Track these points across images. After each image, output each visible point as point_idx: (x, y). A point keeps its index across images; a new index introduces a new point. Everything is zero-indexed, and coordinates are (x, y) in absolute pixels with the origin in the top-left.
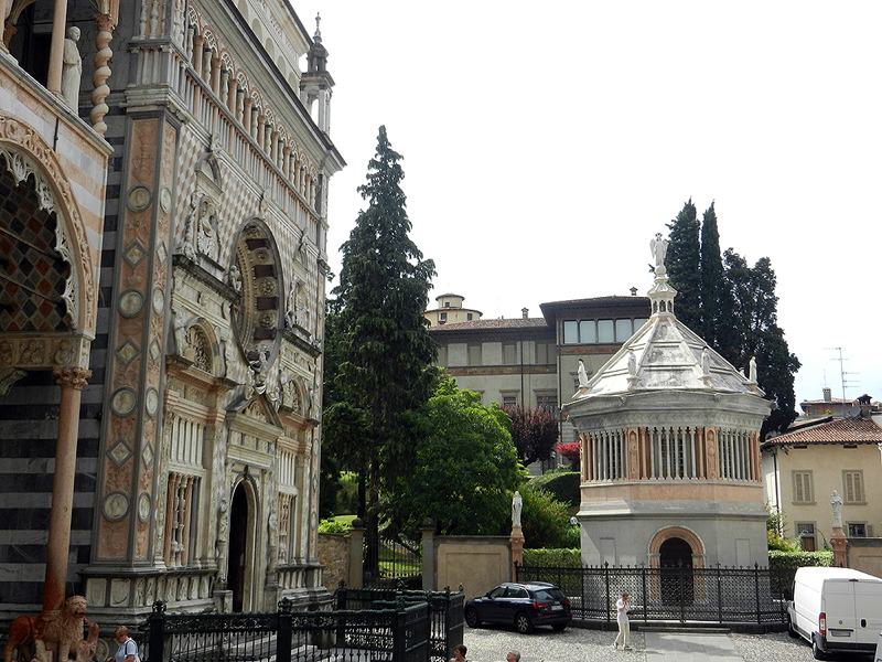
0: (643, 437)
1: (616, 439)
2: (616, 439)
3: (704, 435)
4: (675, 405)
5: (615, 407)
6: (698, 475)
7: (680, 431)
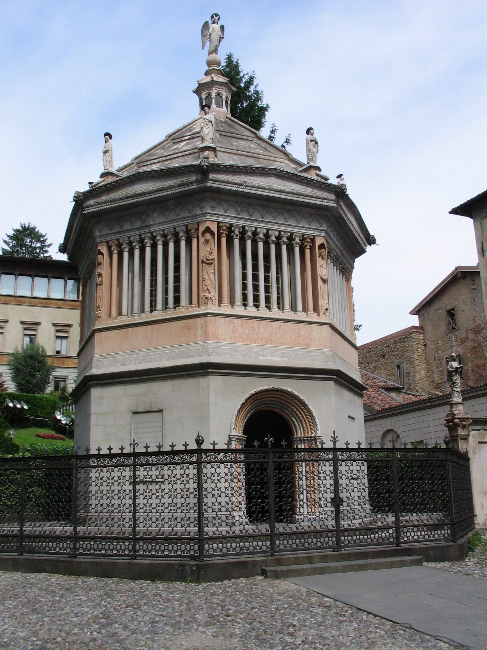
0: (224, 240)
1: (171, 246)
2: (171, 246)
3: (312, 249)
4: (281, 191)
5: (180, 185)
6: (305, 309)
7: (279, 238)
